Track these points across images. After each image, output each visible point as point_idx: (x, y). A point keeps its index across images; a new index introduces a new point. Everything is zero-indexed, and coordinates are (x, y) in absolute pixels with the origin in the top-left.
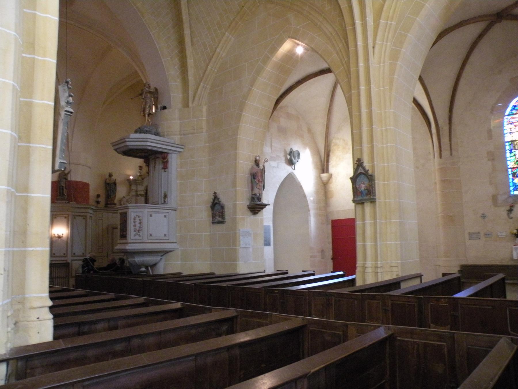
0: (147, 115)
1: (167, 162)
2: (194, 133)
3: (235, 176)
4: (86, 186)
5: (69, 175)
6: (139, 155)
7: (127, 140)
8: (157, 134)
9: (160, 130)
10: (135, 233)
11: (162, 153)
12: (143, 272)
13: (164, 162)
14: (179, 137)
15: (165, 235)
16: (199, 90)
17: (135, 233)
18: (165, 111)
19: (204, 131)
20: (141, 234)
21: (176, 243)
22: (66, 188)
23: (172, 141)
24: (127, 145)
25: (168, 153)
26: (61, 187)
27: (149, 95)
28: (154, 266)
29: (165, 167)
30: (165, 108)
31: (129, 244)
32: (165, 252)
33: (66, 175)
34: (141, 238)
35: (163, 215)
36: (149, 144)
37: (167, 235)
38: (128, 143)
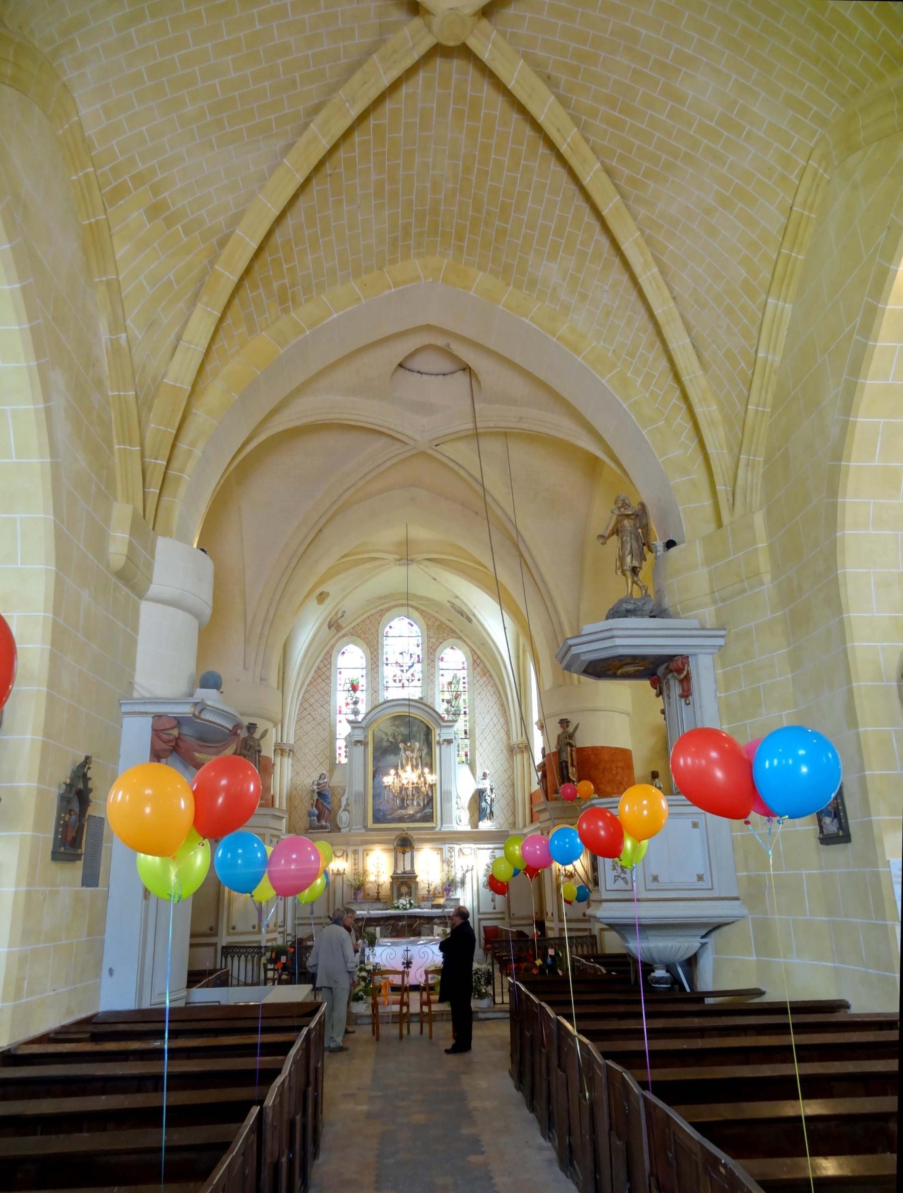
0: (628, 574)
1: (687, 678)
2: (743, 591)
3: (850, 691)
4: (624, 756)
5: (577, 735)
6: (619, 672)
7: (570, 642)
8: (659, 613)
9: (667, 602)
10: (615, 873)
11: (671, 658)
12: (659, 980)
13: (681, 681)
14: (712, 608)
15: (700, 878)
16: (741, 475)
17: (615, 873)
18: (673, 550)
19: (767, 578)
20: (628, 876)
21: (737, 899)
22: (573, 765)
23: (695, 623)
24: (578, 655)
25: (685, 658)
26: (564, 764)
27: (626, 522)
28: (691, 962)
29: (686, 694)
30: (670, 544)
31: (604, 904)
32: (713, 928)
33: (571, 736)
34: (629, 887)
35: (688, 823)
36: (618, 642)
37: (707, 877)
38: (574, 650)
